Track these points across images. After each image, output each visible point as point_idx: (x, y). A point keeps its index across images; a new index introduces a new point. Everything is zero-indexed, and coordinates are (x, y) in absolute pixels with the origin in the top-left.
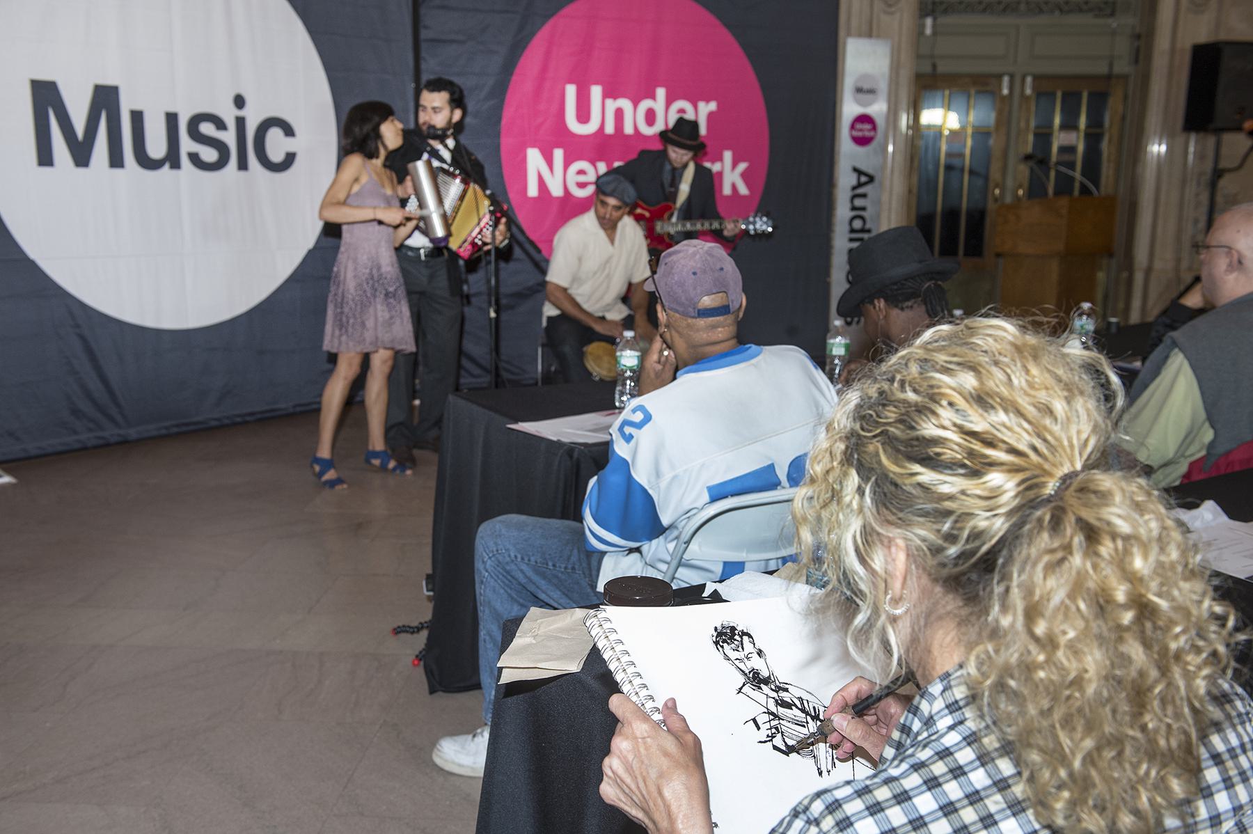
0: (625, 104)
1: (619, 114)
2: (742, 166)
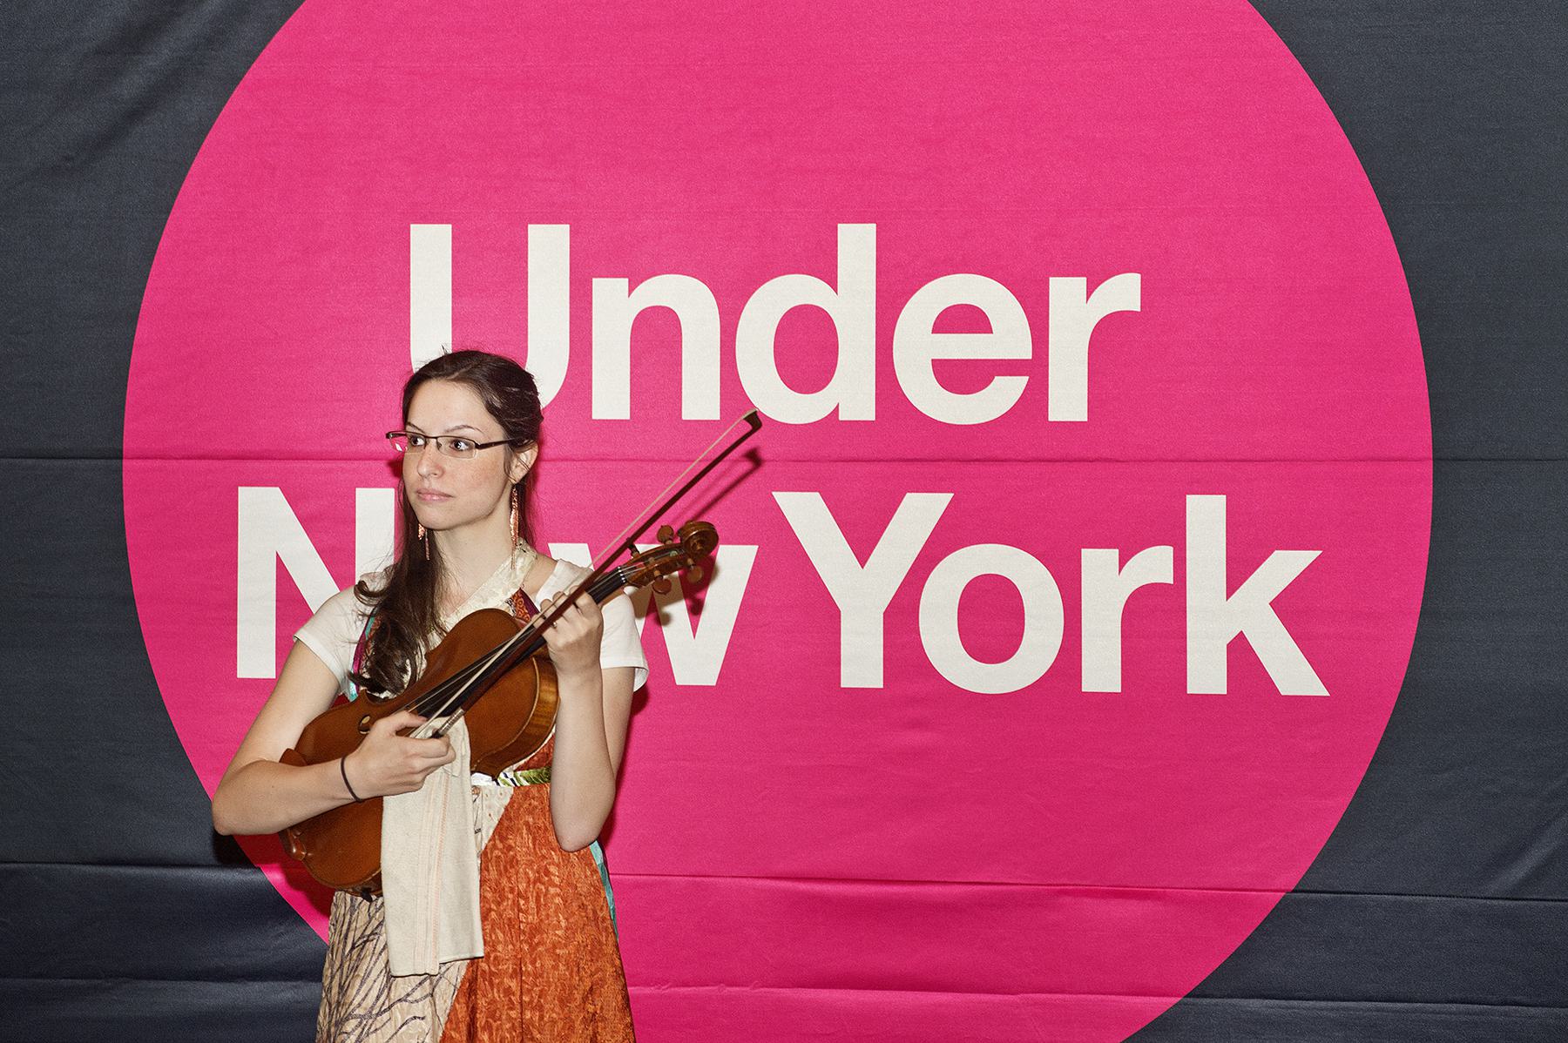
0: (688, 298)
1: (656, 337)
2: (1285, 567)
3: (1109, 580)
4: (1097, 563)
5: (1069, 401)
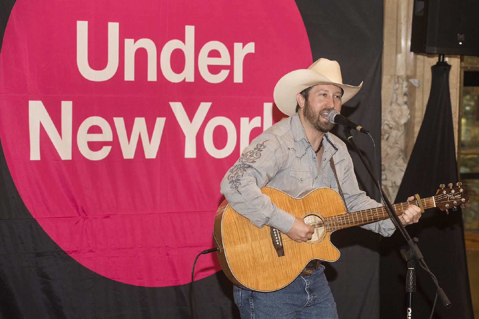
1: (141, 55)
3: (247, 125)
4: (244, 121)
5: (238, 78)
